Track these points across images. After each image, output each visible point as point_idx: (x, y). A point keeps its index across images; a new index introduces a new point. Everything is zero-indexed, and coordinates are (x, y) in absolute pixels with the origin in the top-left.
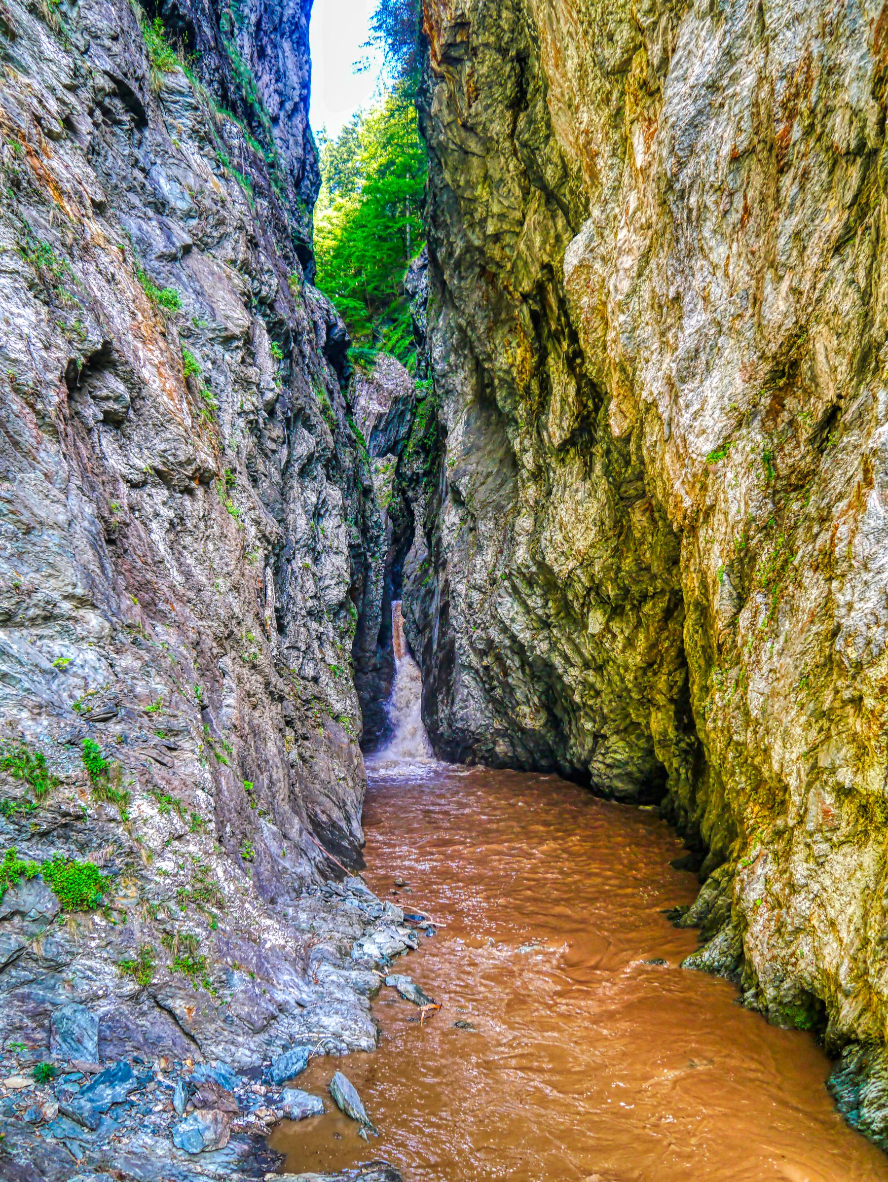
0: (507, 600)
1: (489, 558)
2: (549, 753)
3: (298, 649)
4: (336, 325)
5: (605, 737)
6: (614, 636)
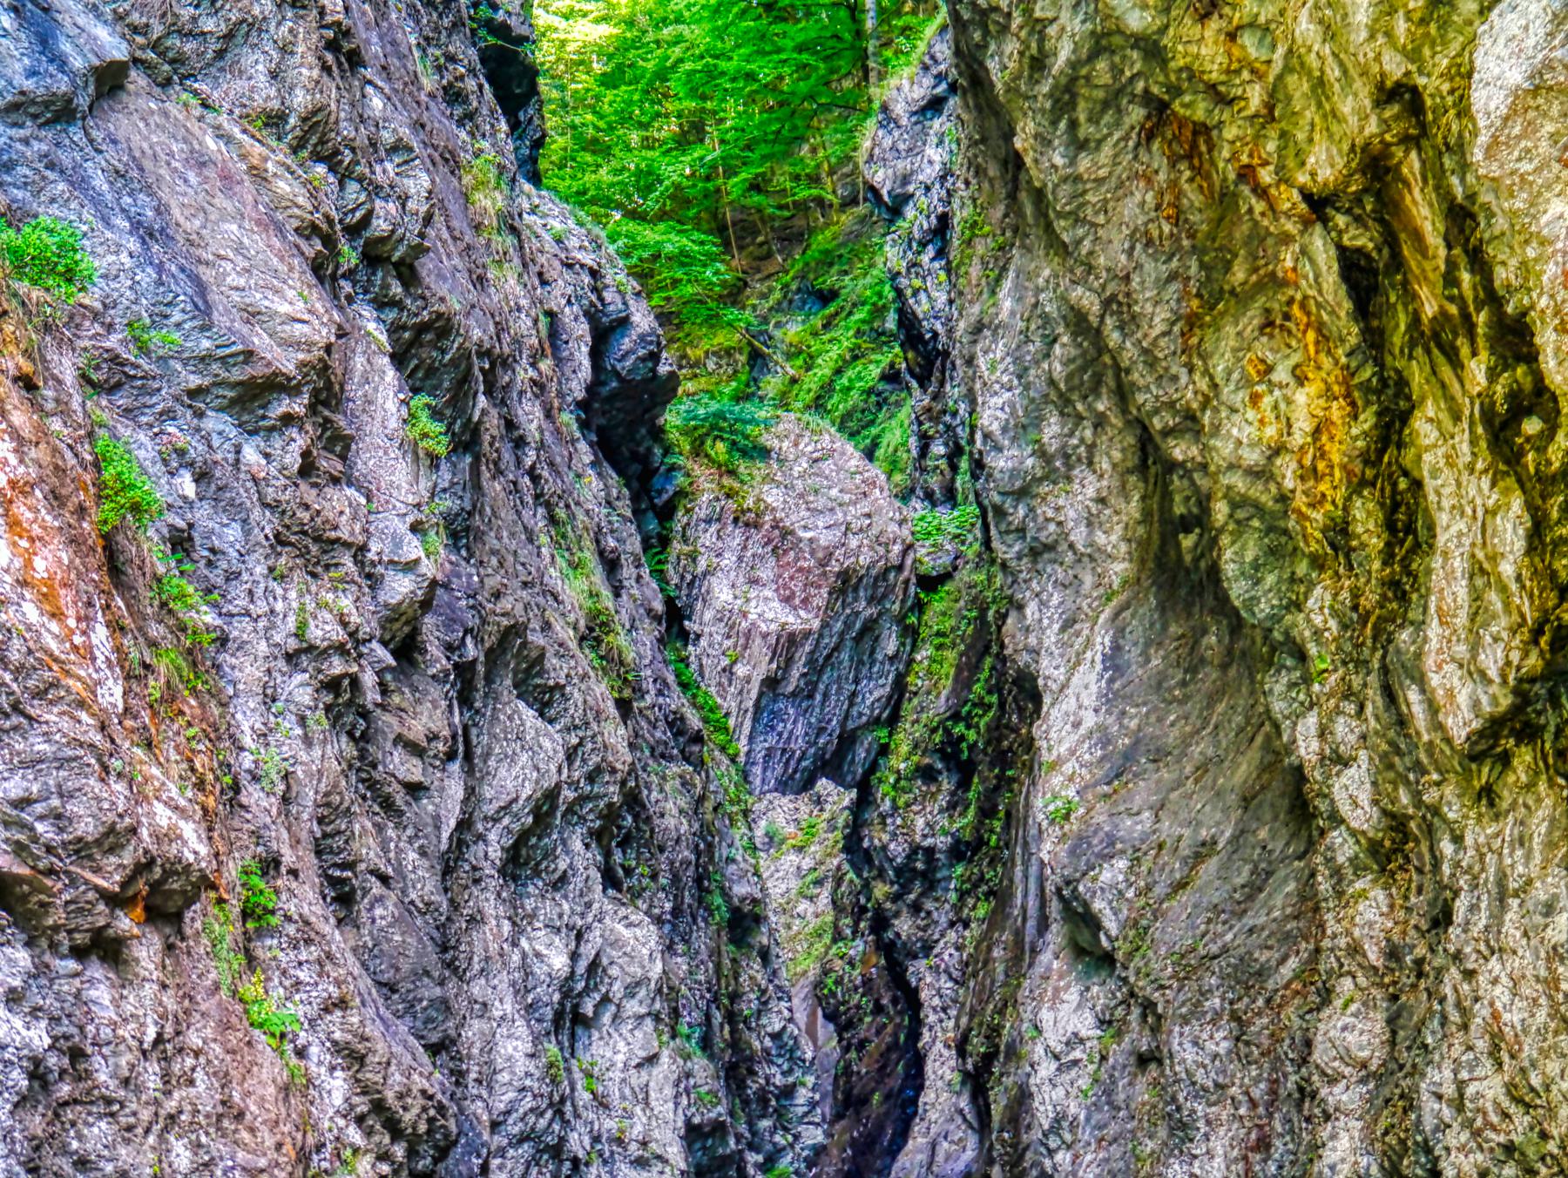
4: (624, 322)
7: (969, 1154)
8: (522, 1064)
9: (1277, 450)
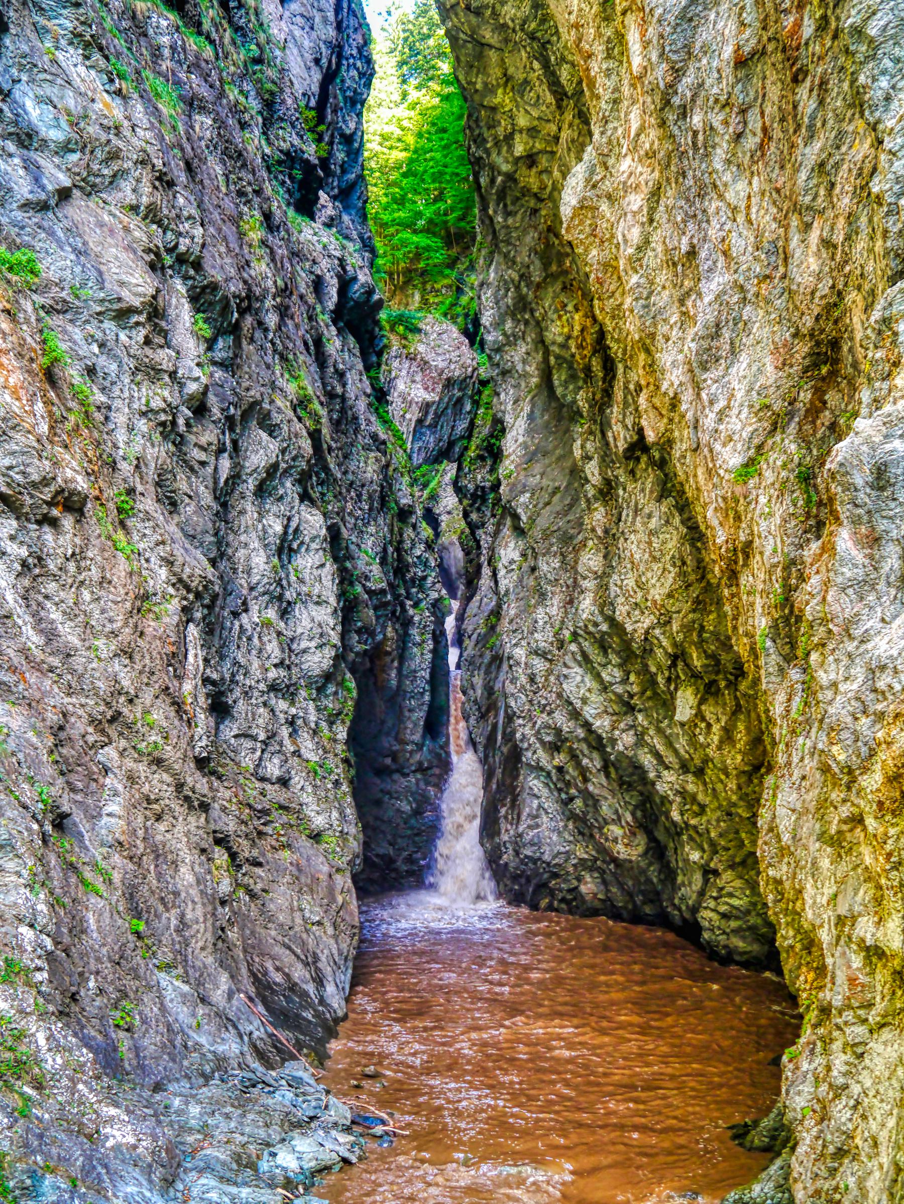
0: (576, 672)
1: (554, 611)
2: (654, 897)
3: (254, 738)
4: (355, 279)
5: (716, 873)
6: (709, 726)
8: (262, 566)
9: (569, 337)
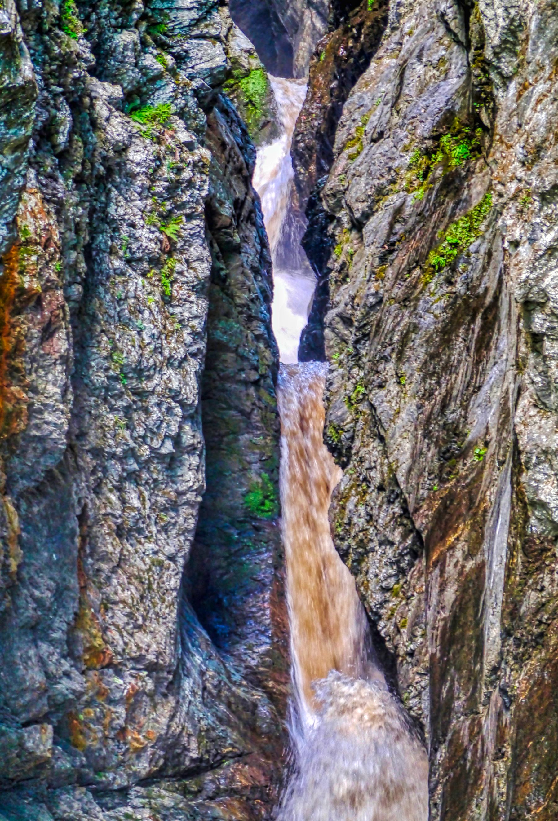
7: (454, 83)
